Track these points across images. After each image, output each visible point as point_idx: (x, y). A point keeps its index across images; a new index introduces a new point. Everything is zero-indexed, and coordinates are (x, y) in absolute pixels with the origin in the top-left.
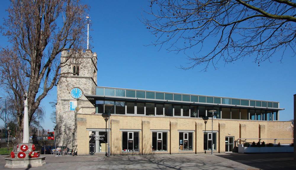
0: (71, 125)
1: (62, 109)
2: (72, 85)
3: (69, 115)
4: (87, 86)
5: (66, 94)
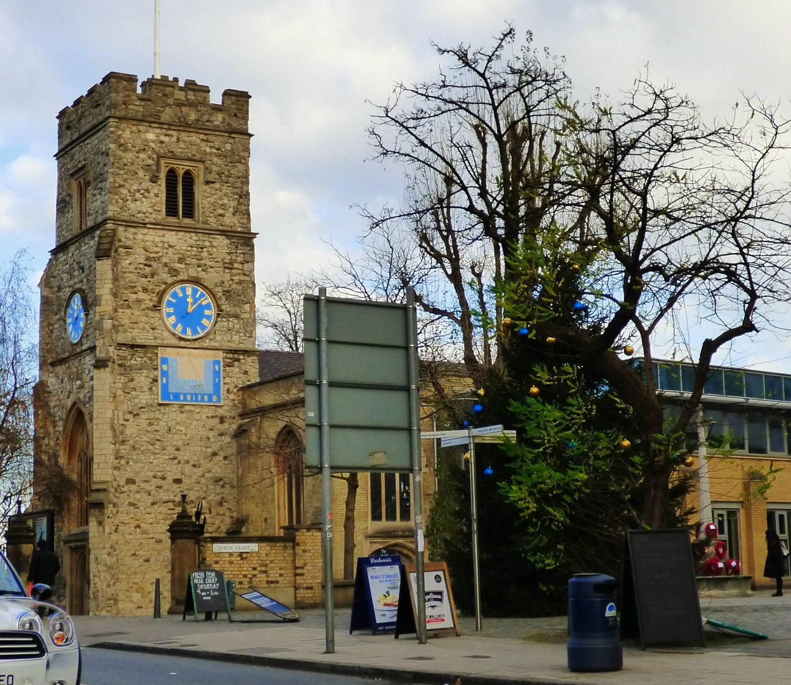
0: (164, 478)
1: (120, 392)
2: (166, 265)
3: (154, 427)
4: (236, 278)
5: (137, 313)
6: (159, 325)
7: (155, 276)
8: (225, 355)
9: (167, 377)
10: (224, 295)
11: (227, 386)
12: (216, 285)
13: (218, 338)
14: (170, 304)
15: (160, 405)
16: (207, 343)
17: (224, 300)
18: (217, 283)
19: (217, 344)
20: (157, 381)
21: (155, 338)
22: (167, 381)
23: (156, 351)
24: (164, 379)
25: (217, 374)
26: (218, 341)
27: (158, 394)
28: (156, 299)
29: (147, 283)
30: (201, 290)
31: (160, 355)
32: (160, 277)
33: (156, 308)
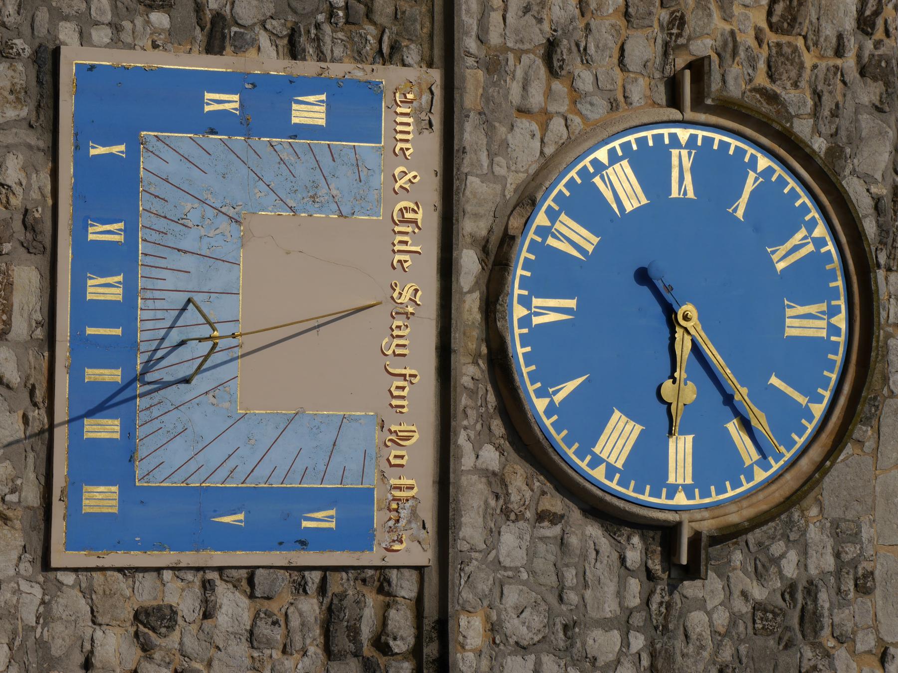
6: (576, 96)
7: (869, 93)
8: (406, 588)
9: (242, 124)
10: (791, 589)
11: (184, 599)
12: (843, 533)
13: (512, 543)
14: (717, 173)
15: (48, 61)
16: (481, 453)
17: (758, 593)
18: (856, 537)
19: (471, 529)
20: (213, 47)
21: (493, 66)
22: (216, 124)
23: (412, 54)
24: (231, 102)
25: (276, 511)
26: (493, 534)
27: (116, 42)
28: (736, 89)
29: (829, 31)
30: (818, 410)
31: (389, 76)
32: (867, 121)
33: (688, 88)
